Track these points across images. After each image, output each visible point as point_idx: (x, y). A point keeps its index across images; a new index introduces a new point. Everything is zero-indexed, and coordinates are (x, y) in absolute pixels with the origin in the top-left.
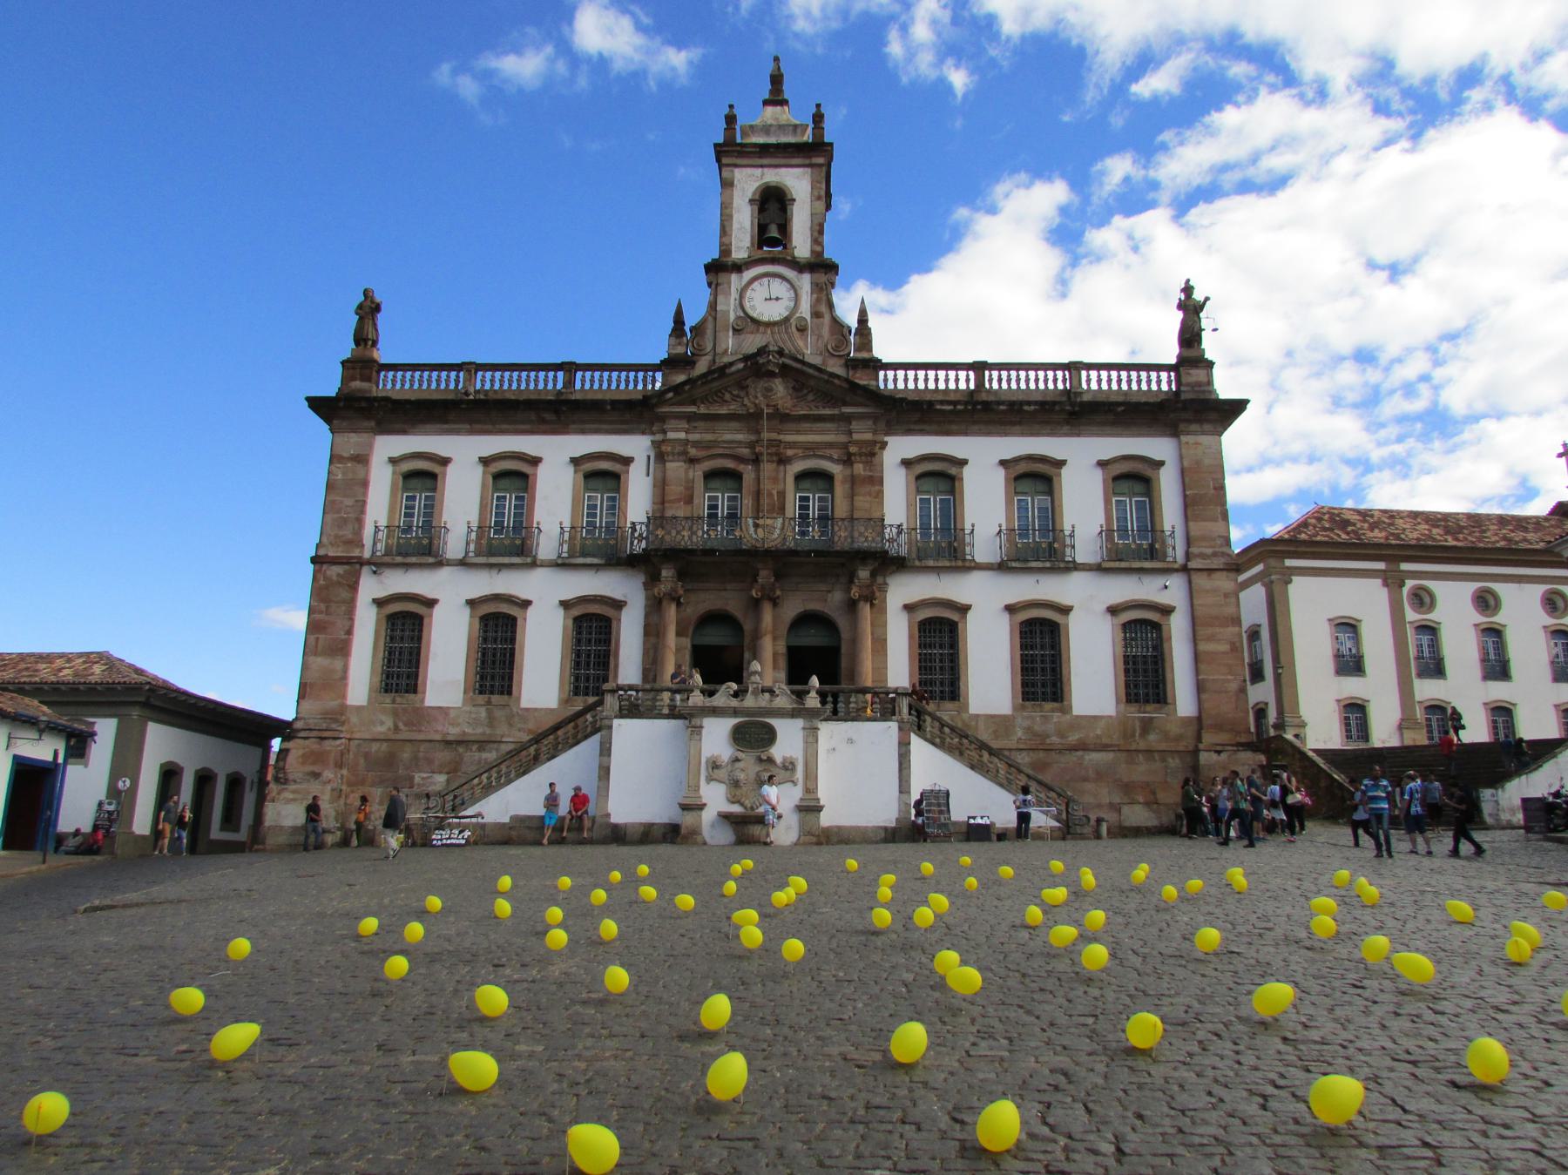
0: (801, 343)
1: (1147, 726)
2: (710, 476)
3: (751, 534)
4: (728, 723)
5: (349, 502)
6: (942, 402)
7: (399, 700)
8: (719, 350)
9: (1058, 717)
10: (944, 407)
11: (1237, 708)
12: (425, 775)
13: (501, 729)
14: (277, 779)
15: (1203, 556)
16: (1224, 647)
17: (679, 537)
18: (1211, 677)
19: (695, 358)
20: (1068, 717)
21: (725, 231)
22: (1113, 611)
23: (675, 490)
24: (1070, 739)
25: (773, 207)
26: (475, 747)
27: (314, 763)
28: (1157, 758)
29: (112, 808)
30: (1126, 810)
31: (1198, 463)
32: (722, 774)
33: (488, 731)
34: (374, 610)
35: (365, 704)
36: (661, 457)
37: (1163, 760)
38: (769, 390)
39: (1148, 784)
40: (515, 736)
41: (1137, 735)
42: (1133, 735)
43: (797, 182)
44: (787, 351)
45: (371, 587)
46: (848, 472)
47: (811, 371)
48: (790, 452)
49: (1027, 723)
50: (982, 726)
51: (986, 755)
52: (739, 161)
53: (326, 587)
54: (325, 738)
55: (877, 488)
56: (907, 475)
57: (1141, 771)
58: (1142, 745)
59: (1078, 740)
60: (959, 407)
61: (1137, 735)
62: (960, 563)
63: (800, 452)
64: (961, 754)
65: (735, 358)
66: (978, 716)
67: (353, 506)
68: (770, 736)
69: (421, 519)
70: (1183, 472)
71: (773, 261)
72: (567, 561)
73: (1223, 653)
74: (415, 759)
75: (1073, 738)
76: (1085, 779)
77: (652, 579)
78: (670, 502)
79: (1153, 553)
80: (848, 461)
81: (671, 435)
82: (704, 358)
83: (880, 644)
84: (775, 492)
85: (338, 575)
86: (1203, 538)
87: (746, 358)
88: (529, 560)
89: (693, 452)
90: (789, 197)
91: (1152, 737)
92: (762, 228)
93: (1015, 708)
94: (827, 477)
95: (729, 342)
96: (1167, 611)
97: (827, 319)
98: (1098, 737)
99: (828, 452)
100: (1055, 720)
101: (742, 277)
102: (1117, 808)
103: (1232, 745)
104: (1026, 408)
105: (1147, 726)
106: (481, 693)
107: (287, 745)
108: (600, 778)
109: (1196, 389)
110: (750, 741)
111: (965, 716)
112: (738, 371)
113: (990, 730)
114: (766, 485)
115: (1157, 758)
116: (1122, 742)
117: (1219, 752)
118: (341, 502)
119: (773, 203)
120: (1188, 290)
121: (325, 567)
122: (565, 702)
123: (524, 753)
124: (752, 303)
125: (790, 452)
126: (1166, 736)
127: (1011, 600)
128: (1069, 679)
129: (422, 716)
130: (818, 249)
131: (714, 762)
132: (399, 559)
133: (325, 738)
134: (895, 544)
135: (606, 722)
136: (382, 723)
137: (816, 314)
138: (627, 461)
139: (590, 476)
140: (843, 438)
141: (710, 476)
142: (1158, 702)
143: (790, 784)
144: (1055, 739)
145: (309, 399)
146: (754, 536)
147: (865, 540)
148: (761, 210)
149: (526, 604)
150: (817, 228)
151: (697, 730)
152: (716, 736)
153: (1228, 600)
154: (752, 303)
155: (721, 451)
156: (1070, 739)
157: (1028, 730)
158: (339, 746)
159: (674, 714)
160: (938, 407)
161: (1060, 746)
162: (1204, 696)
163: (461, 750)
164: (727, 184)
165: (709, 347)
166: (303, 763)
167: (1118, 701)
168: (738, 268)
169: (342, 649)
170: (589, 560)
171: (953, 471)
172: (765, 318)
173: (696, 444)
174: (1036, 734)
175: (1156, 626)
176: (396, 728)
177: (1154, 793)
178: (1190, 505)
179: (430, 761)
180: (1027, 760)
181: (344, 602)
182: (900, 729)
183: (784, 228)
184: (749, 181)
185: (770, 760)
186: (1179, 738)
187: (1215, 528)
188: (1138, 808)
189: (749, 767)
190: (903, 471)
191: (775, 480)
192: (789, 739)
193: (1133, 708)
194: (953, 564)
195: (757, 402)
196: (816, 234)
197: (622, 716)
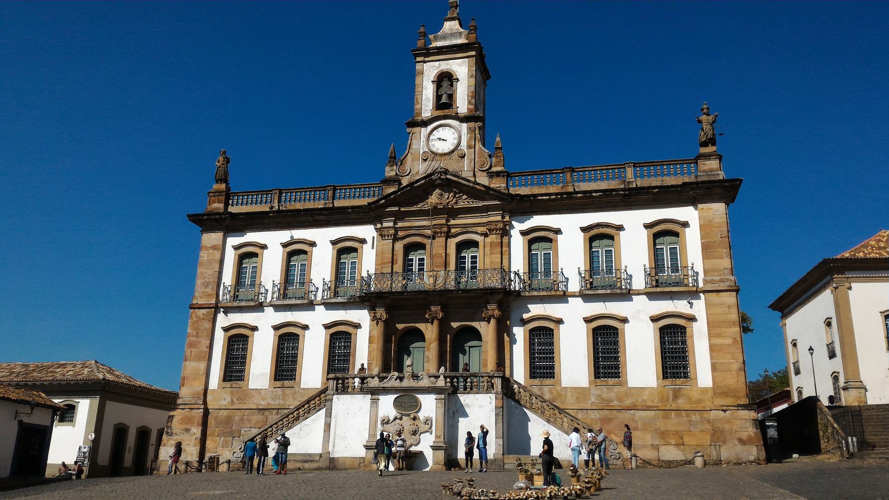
4: (392, 397)
6: (542, 195)
7: (234, 386)
8: (413, 172)
9: (618, 388)
10: (543, 198)
11: (738, 381)
12: (247, 429)
14: (167, 433)
15: (712, 282)
16: (729, 341)
17: (385, 285)
18: (719, 361)
19: (401, 178)
20: (625, 388)
22: (654, 319)
24: (626, 403)
25: (445, 84)
26: (275, 411)
27: (187, 424)
28: (684, 415)
29: (85, 450)
33: (282, 402)
34: (222, 333)
35: (216, 388)
37: (688, 416)
38: (441, 195)
39: (677, 432)
40: (293, 403)
41: (671, 399)
42: (668, 400)
44: (450, 171)
45: (223, 320)
46: (488, 239)
47: (463, 182)
48: (453, 230)
49: (598, 392)
50: (569, 394)
51: (557, 412)
52: (426, 59)
53: (197, 322)
54: (193, 409)
56: (523, 240)
57: (673, 423)
58: (674, 406)
59: (630, 404)
60: (555, 197)
61: (671, 399)
62: (553, 293)
63: (459, 229)
64: (543, 413)
65: (417, 178)
66: (566, 388)
67: (212, 275)
68: (417, 406)
69: (250, 280)
70: (702, 227)
72: (326, 301)
73: (727, 345)
74: (242, 420)
75: (628, 402)
77: (372, 309)
78: (384, 263)
81: (385, 225)
82: (405, 177)
84: (444, 255)
85: (203, 314)
88: (306, 301)
90: (454, 78)
92: (438, 97)
93: (590, 383)
94: (475, 244)
98: (645, 401)
99: (474, 229)
100: (616, 390)
101: (426, 129)
102: (656, 448)
103: (734, 406)
104: (594, 194)
107: (172, 413)
108: (325, 431)
109: (709, 173)
110: (404, 407)
111: (558, 388)
112: (422, 184)
113: (575, 397)
115: (684, 415)
116: (660, 405)
117: (725, 411)
118: (206, 272)
119: (445, 79)
121: (196, 310)
123: (291, 416)
124: (433, 143)
126: (689, 399)
127: (588, 314)
128: (625, 364)
129: (248, 394)
131: (384, 420)
132: (235, 304)
133: (193, 409)
134: (512, 283)
135: (329, 397)
136: (225, 399)
137: (469, 147)
138: (363, 241)
139: (341, 252)
140: (485, 220)
141: (409, 248)
142: (685, 377)
143: (428, 433)
144: (615, 403)
145: (188, 216)
146: (428, 283)
147: (494, 282)
150: (471, 94)
151: (375, 402)
152: (387, 405)
153: (730, 310)
154: (433, 143)
155: (412, 232)
156: (626, 403)
158: (200, 413)
159: (363, 391)
160: (540, 198)
161: (619, 408)
162: (714, 374)
163: (267, 413)
166: (181, 424)
167: (658, 379)
168: (425, 123)
169: (204, 357)
170: (339, 300)
171: (551, 235)
174: (604, 400)
175: (682, 330)
176: (232, 402)
177: (682, 438)
178: (707, 249)
179: (250, 421)
180: (598, 416)
181: (206, 329)
182: (496, 398)
183: (451, 97)
186: (699, 401)
190: (521, 238)
193: (668, 382)
194: (549, 293)
195: (434, 202)
196: (470, 98)
197: (338, 394)
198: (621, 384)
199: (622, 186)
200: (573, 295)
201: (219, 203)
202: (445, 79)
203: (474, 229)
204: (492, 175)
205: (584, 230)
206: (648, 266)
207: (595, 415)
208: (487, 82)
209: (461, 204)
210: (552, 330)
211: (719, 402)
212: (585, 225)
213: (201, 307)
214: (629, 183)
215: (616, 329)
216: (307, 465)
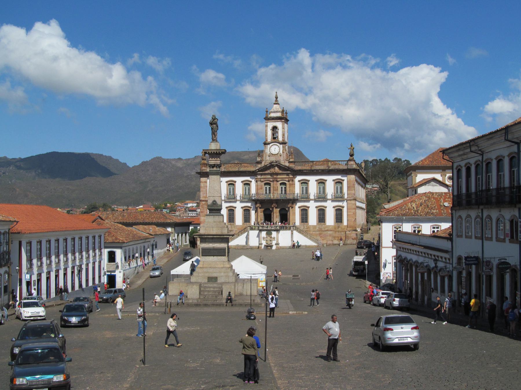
0: (280, 158)
1: (339, 227)
2: (265, 184)
3: (272, 196)
5: (205, 190)
6: (305, 170)
13: (233, 229)
21: (266, 136)
22: (334, 207)
23: (259, 187)
30: (334, 241)
31: (350, 180)
32: (265, 239)
36: (257, 182)
37: (341, 233)
43: (279, 124)
48: (279, 180)
50: (311, 227)
55: (293, 186)
57: (337, 234)
63: (280, 179)
65: (268, 164)
68: (271, 234)
71: (275, 142)
75: (326, 229)
76: (328, 236)
77: (256, 204)
79: (342, 197)
80: (289, 181)
81: (258, 177)
83: (294, 214)
86: (349, 194)
87: (270, 164)
89: (262, 180)
91: (339, 229)
92: (273, 135)
95: (268, 158)
96: (343, 207)
97: (285, 153)
99: (285, 179)
105: (339, 227)
106: (229, 222)
114: (275, 186)
119: (275, 128)
120: (351, 146)
122: (243, 224)
125: (279, 180)
126: (342, 228)
130: (283, 139)
137: (283, 152)
138: (251, 182)
139: (245, 184)
144: (323, 229)
147: (291, 197)
148: (273, 130)
149: (235, 208)
152: (264, 234)
157: (319, 228)
164: (267, 126)
165: (264, 159)
168: (269, 144)
170: (245, 200)
171: (307, 182)
172: (274, 153)
173: (262, 178)
174: (320, 229)
178: (349, 188)
184: (271, 125)
185: (271, 237)
186: (344, 229)
187: (353, 192)
188: (336, 241)
189: (269, 238)
191: (276, 185)
192: (274, 234)
193: (337, 223)
198: (325, 225)
199: (327, 168)
200: (312, 200)
201: (205, 167)
202: (275, 128)
203: (285, 179)
204: (290, 162)
205: (316, 181)
206: (333, 192)
207: (318, 233)
208: (288, 122)
209: (281, 172)
210: (307, 210)
211: (348, 229)
212: (317, 179)
213: (203, 201)
214: (330, 167)
215: (324, 210)
216: (244, 248)
